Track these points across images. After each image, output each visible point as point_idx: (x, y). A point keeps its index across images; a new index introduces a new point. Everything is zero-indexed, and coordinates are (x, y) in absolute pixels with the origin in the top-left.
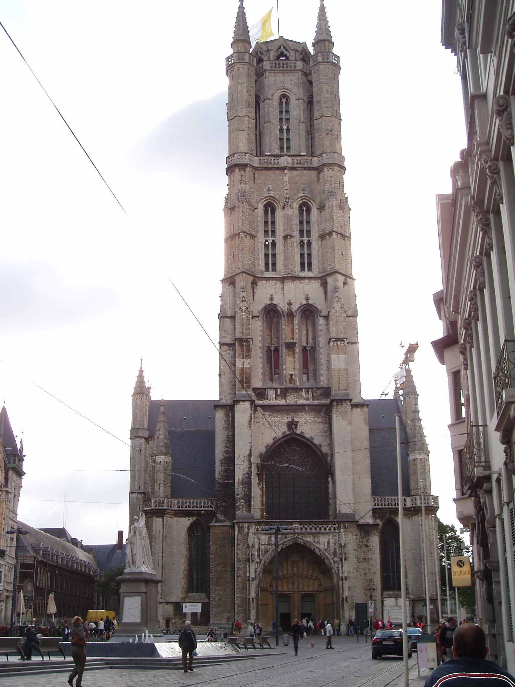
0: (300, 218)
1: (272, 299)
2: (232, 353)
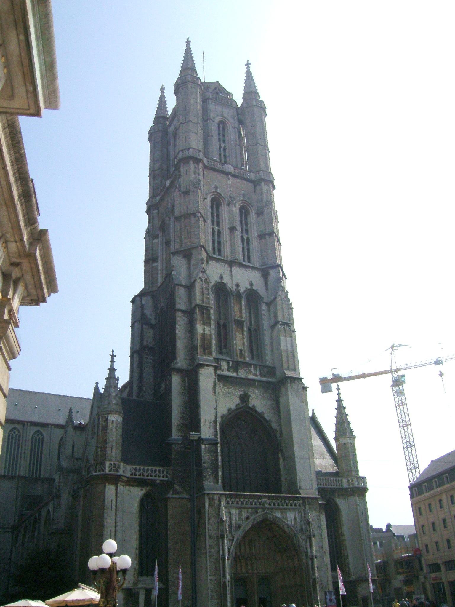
1: (221, 278)
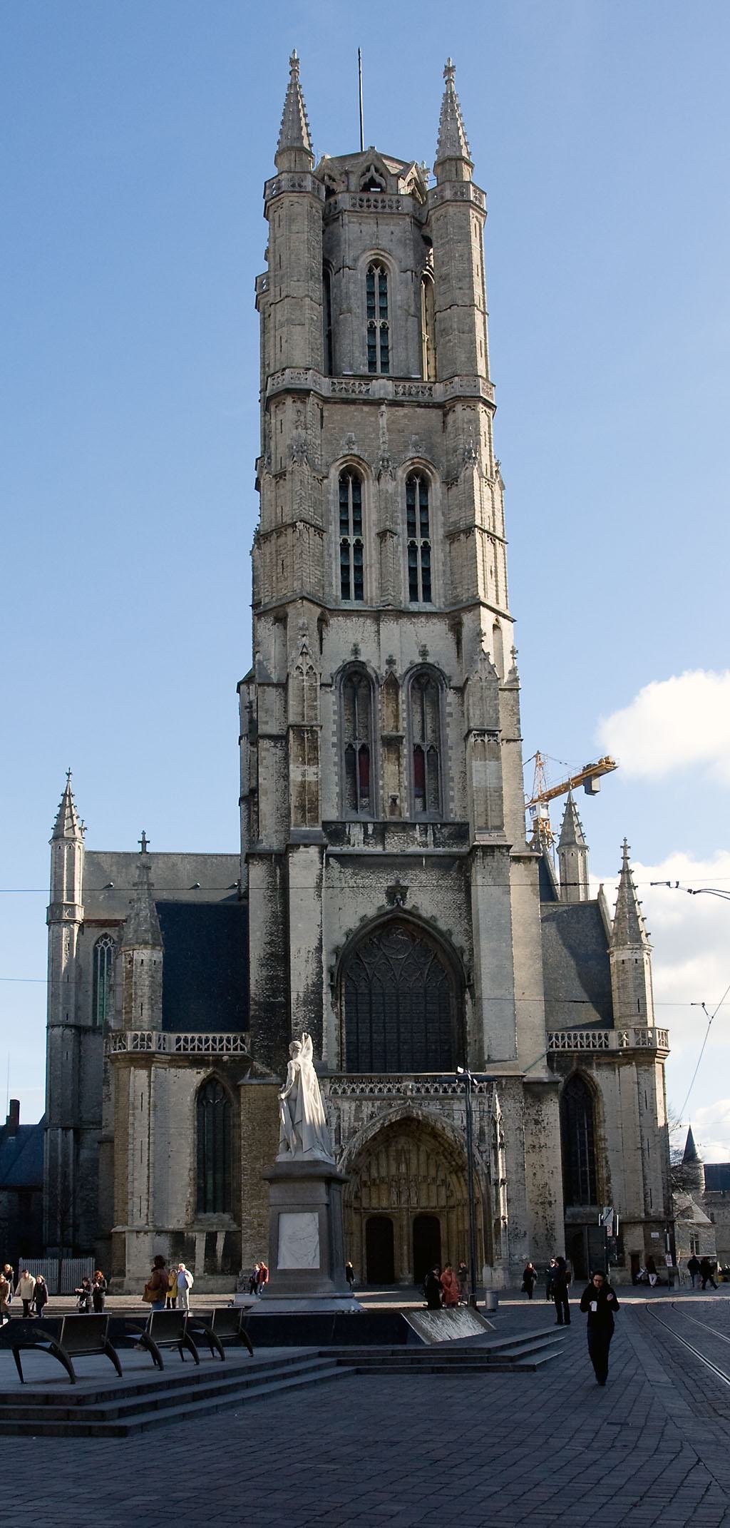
0: (407, 500)
1: (356, 651)
2: (280, 753)
